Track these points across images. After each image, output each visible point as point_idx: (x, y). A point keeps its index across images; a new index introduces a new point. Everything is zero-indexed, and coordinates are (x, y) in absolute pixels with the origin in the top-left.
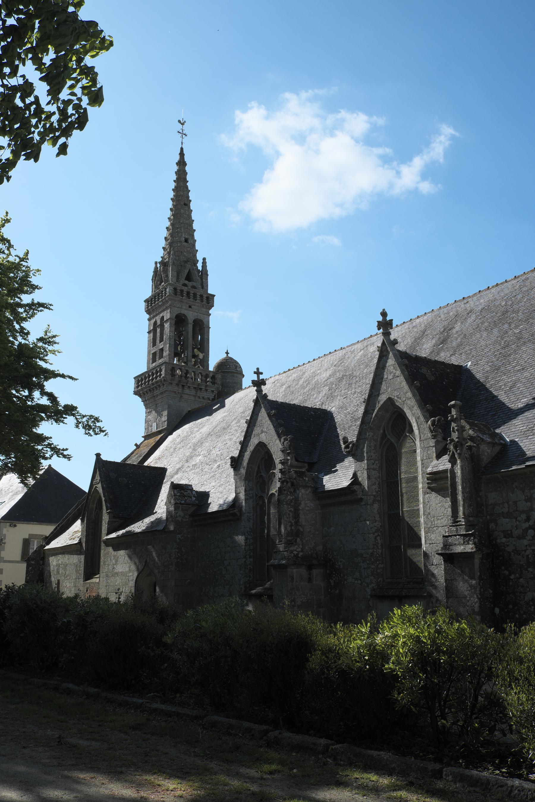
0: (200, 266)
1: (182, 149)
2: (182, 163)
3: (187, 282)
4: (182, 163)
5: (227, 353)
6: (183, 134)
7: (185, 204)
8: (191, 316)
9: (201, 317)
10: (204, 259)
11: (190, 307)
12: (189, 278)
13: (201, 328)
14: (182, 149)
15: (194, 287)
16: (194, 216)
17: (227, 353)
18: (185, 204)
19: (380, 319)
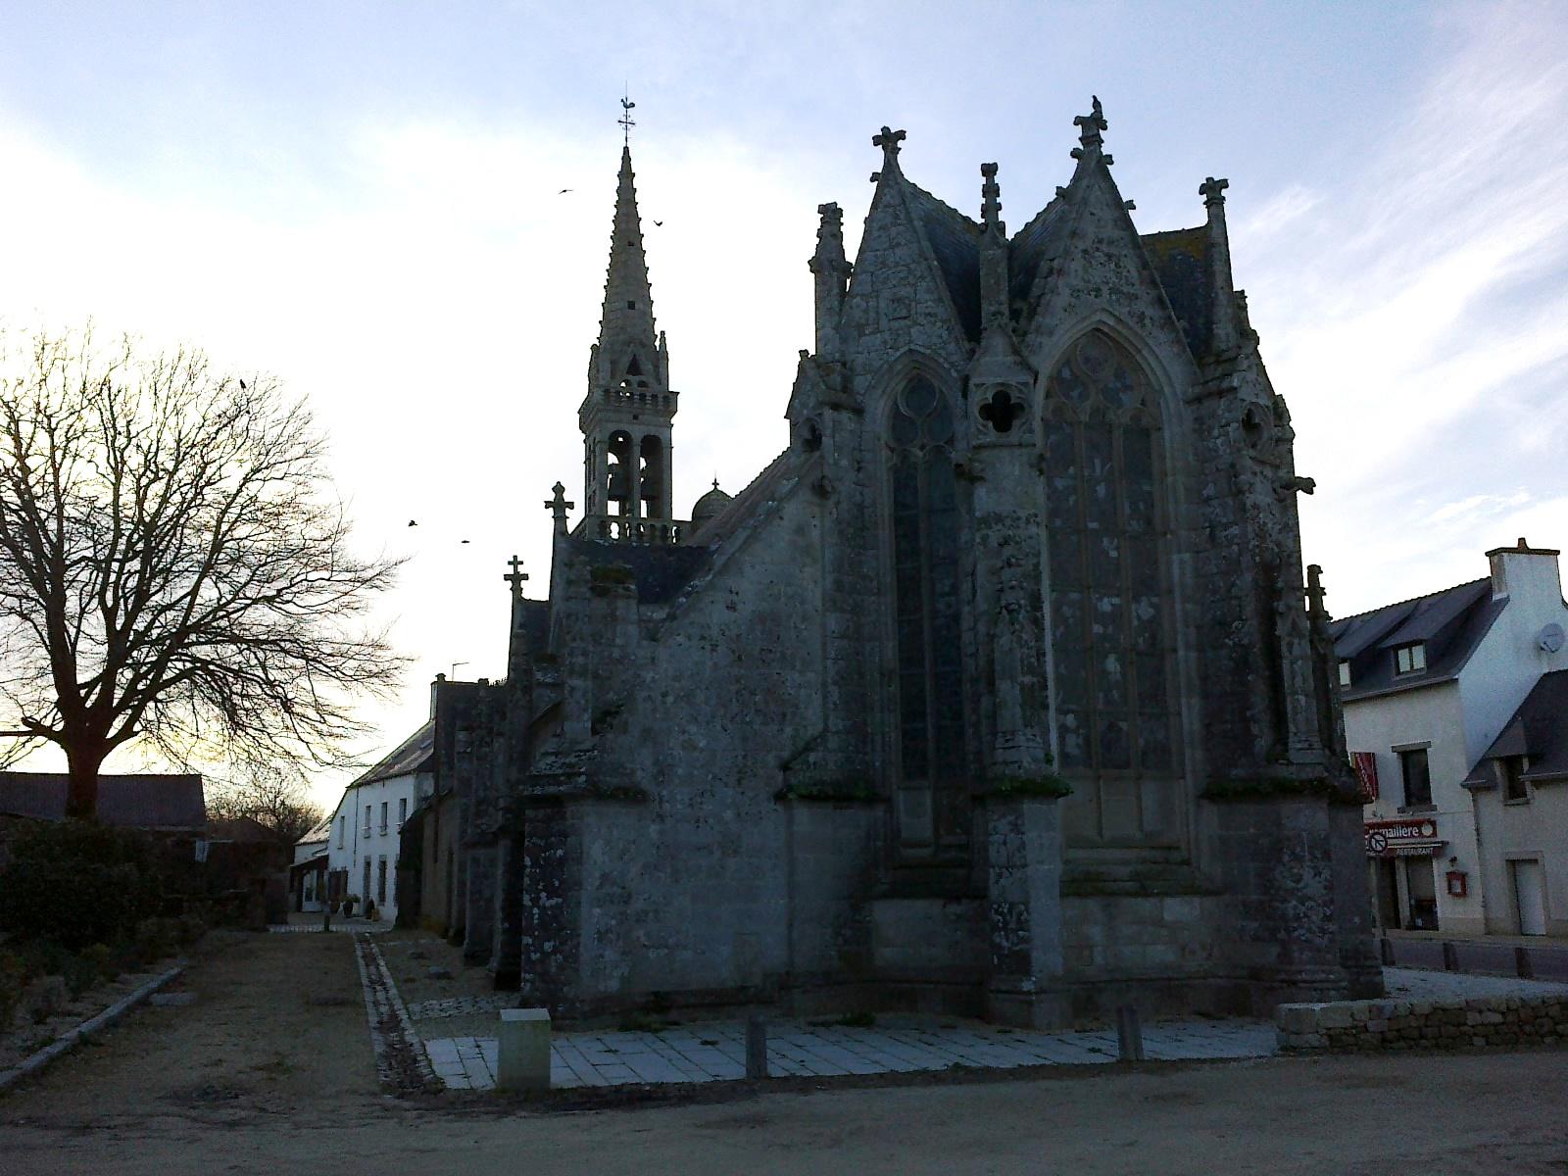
0: (657, 343)
1: (626, 150)
2: (626, 175)
3: (630, 377)
4: (626, 175)
5: (715, 484)
6: (627, 123)
7: (631, 244)
8: (637, 432)
9: (653, 431)
10: (663, 333)
11: (635, 417)
12: (634, 368)
13: (658, 449)
14: (626, 150)
15: (642, 384)
16: (648, 261)
17: (715, 484)
18: (631, 244)
19: (551, 497)
